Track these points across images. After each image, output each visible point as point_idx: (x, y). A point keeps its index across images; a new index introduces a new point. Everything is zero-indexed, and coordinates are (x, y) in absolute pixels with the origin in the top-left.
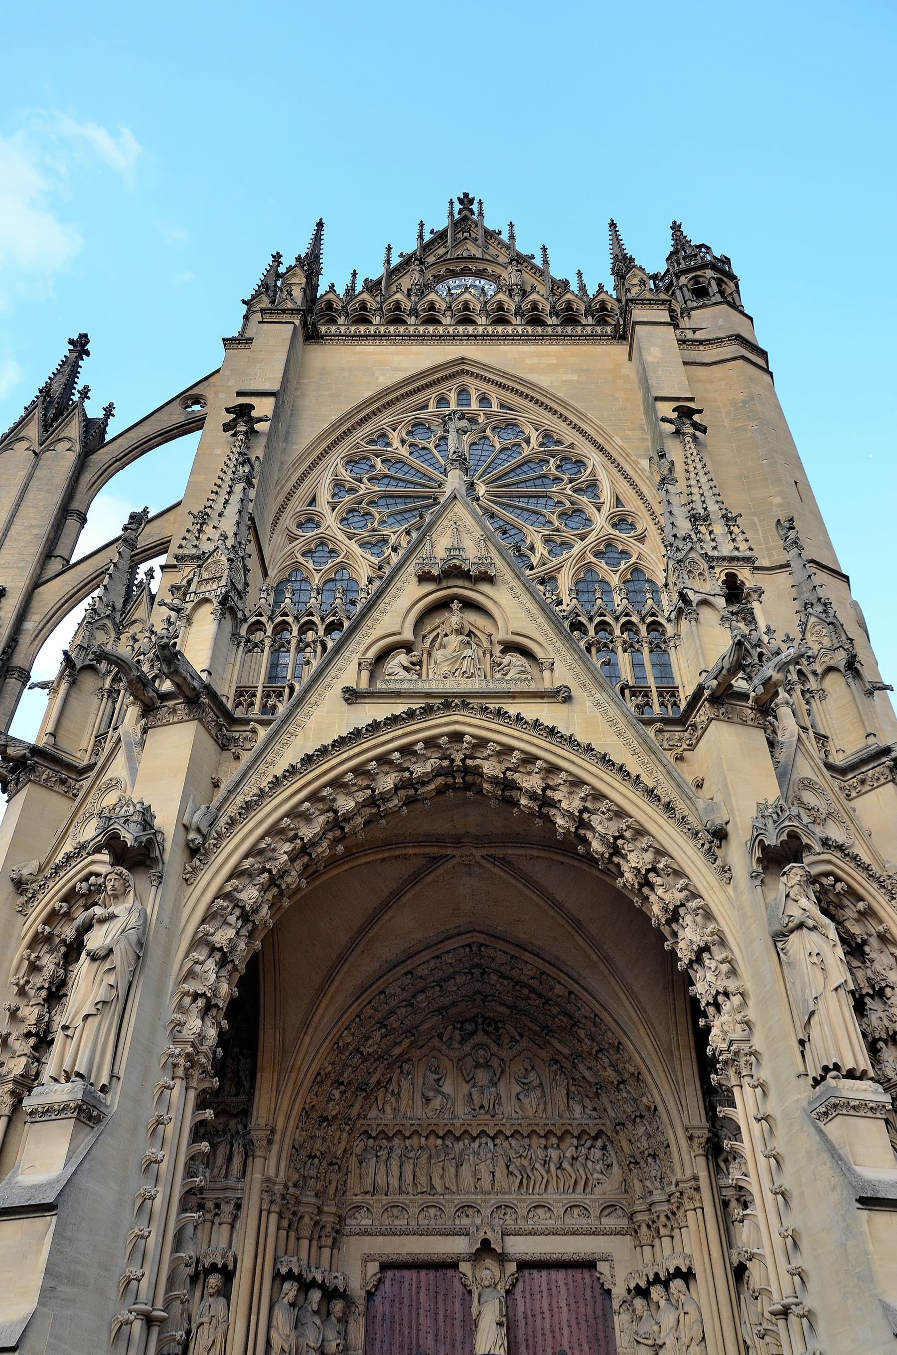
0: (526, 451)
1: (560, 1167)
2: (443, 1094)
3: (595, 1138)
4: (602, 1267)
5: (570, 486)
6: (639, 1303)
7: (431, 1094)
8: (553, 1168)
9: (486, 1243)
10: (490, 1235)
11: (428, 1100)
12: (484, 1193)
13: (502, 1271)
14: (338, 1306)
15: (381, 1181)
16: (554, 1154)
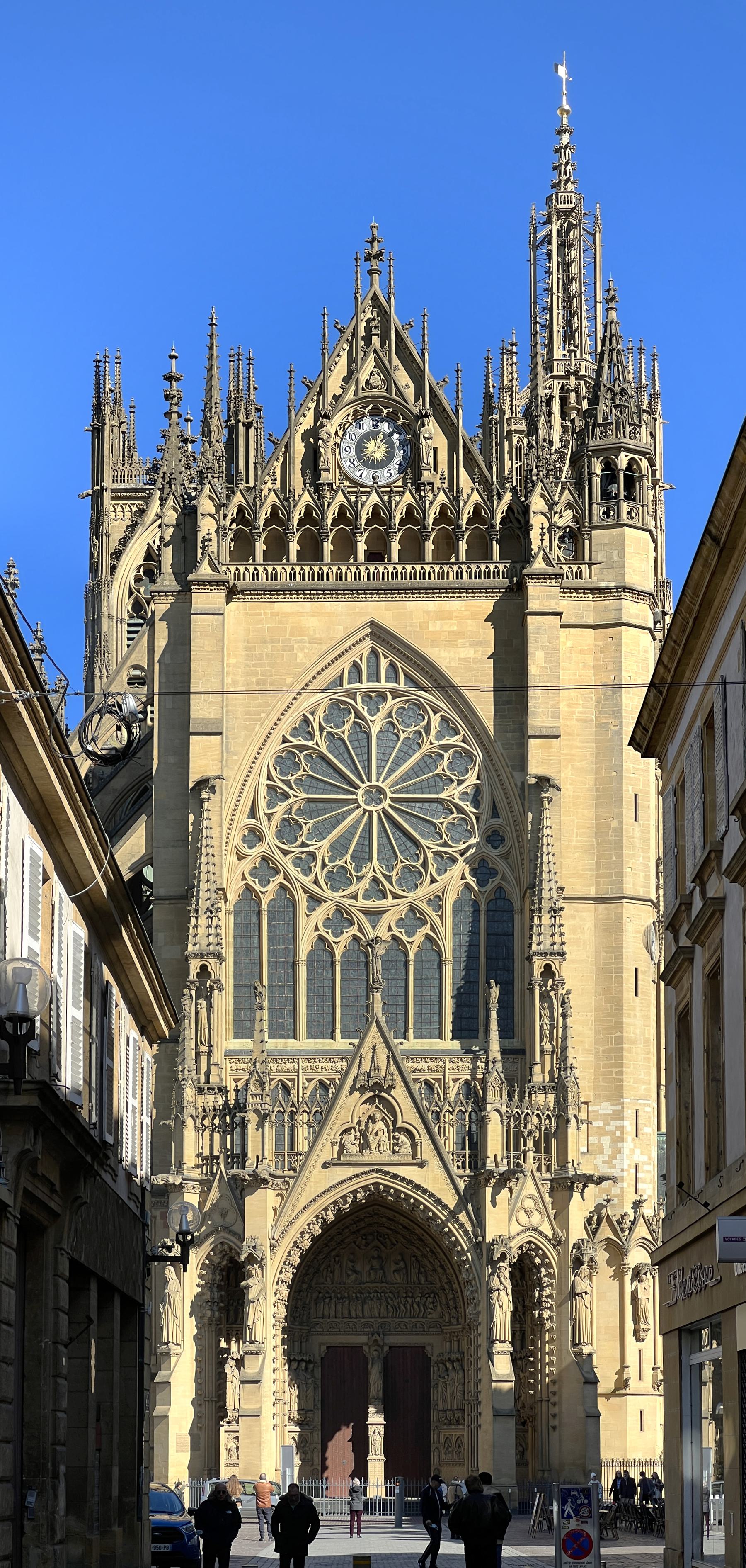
0: (426, 748)
1: (412, 1305)
2: (355, 1272)
3: (429, 1294)
4: (428, 1349)
5: (456, 792)
6: (441, 1366)
7: (350, 1273)
8: (409, 1307)
9: (376, 1341)
10: (378, 1338)
11: (348, 1276)
12: (375, 1317)
13: (382, 1350)
14: (311, 1366)
15: (326, 1313)
16: (409, 1300)
